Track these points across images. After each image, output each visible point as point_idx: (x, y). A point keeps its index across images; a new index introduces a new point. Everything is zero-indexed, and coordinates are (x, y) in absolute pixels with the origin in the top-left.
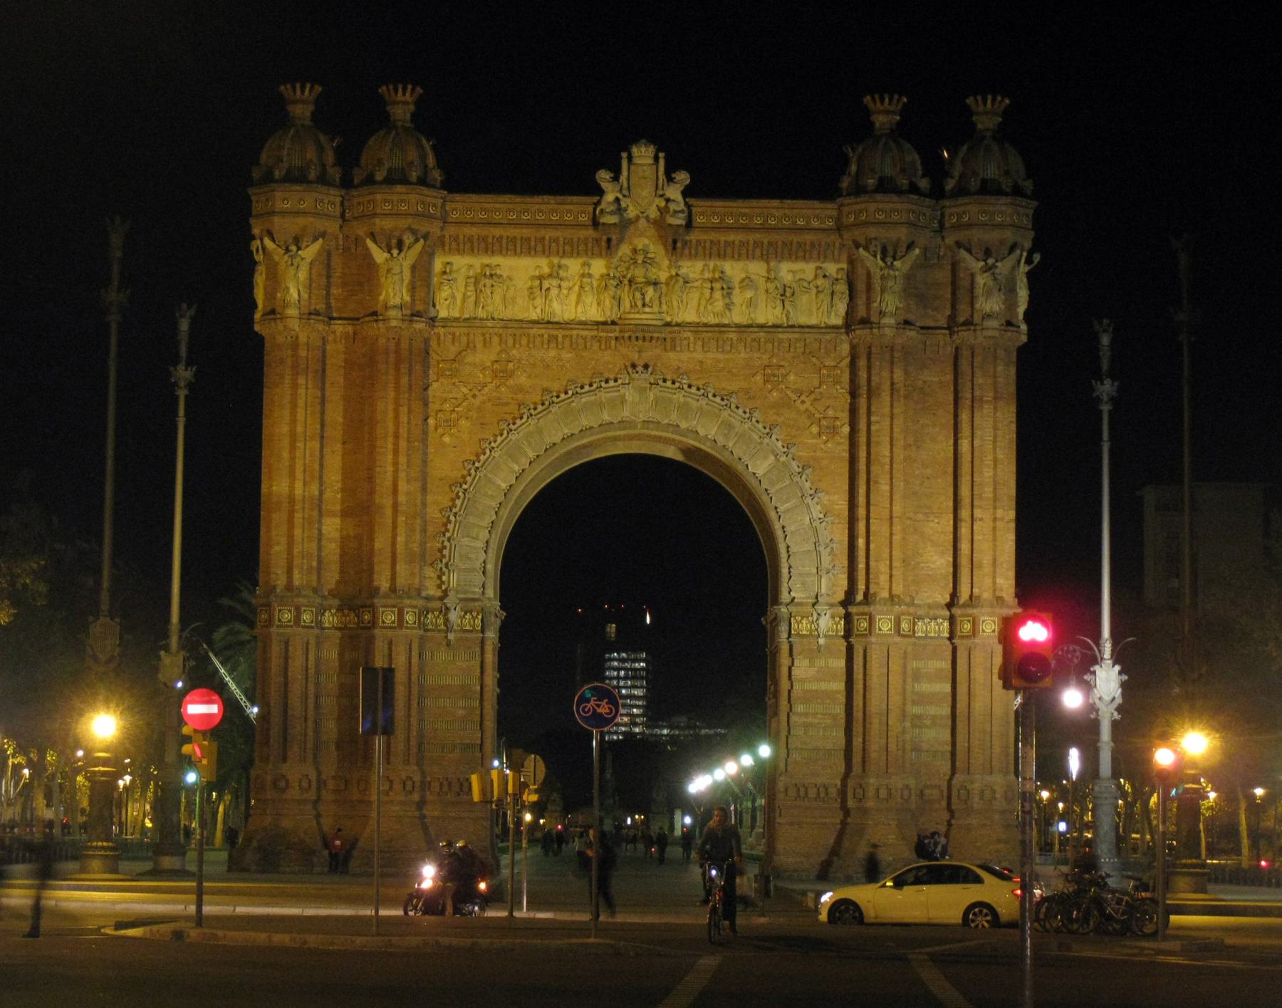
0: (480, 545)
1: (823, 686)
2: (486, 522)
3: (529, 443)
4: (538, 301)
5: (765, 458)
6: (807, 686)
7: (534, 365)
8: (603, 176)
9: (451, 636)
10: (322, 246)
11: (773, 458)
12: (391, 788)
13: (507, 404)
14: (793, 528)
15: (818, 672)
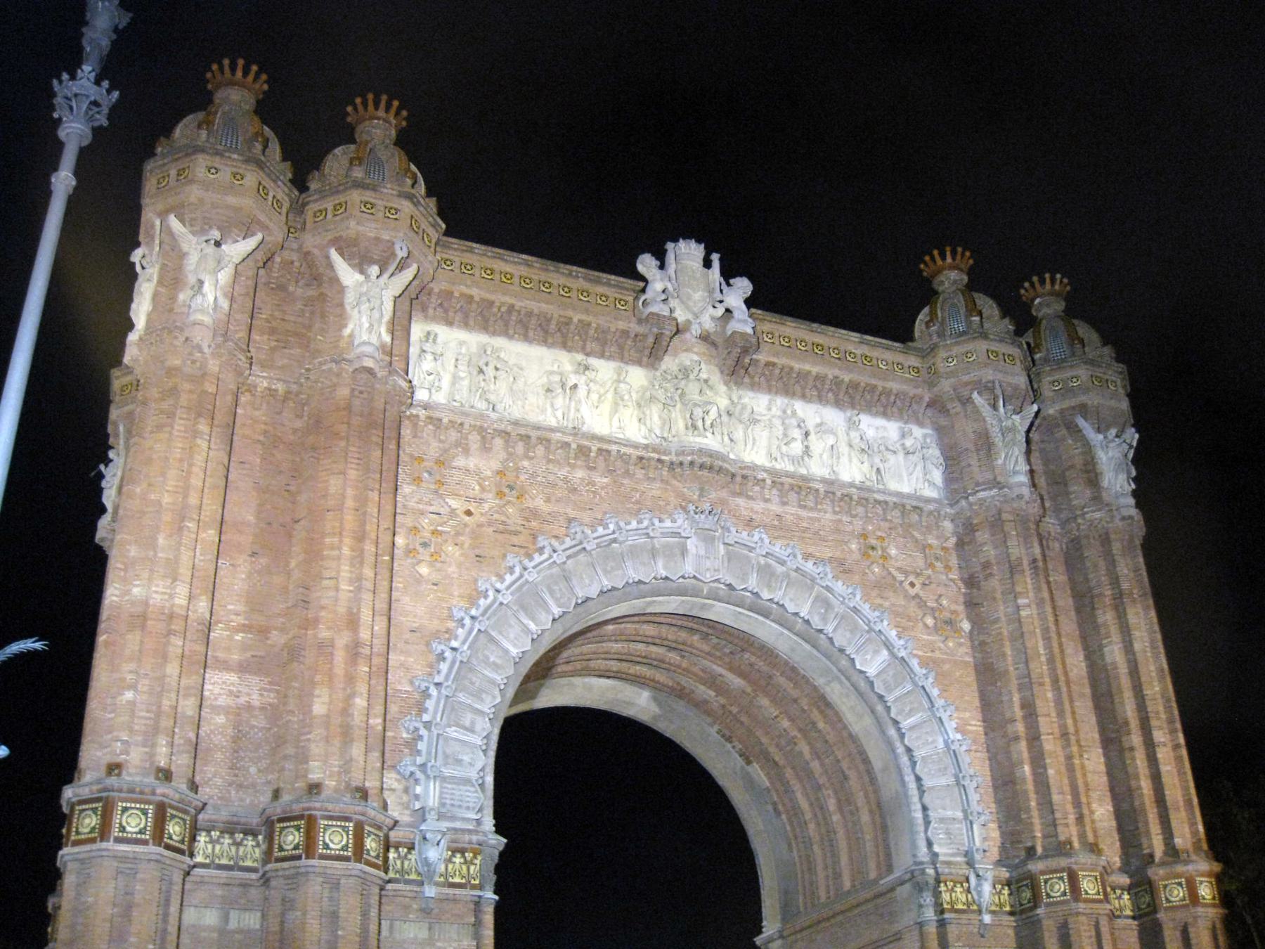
3: (552, 592)
4: (560, 401)
5: (876, 652)
7: (554, 485)
8: (646, 264)
9: (430, 891)
11: (885, 652)
13: (516, 533)
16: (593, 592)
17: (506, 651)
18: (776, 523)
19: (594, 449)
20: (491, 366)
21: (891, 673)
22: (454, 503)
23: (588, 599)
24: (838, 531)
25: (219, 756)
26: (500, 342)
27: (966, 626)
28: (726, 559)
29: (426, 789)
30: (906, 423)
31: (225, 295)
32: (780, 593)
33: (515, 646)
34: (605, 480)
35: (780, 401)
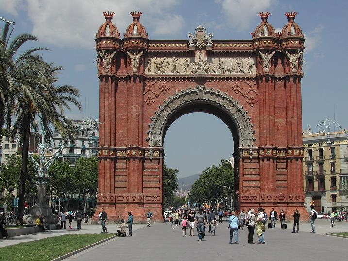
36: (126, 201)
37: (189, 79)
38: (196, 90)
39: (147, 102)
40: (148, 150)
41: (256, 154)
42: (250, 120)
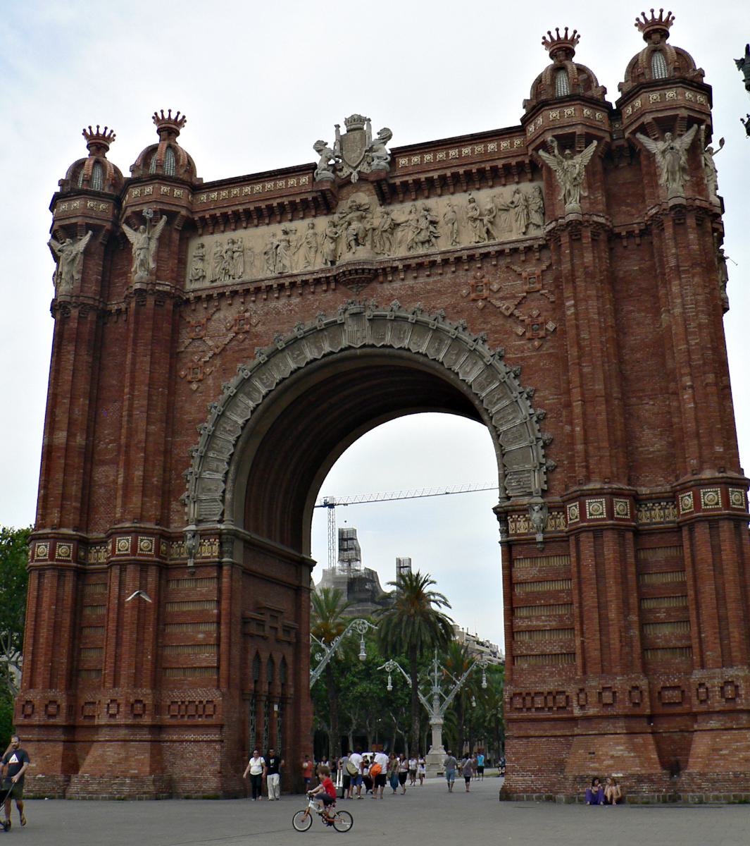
0: (220, 476)
1: (546, 587)
2: (226, 456)
3: (261, 380)
6: (528, 588)
10: (92, 237)
12: (118, 712)
14: (504, 428)
15: (540, 571)
16: (287, 374)
17: (236, 422)
18: (409, 293)
19: (287, 284)
20: (229, 253)
21: (485, 376)
22: (210, 343)
23: (284, 379)
24: (455, 285)
25: (102, 509)
26: (240, 234)
27: (551, 326)
28: (370, 329)
29: (190, 510)
30: (518, 183)
31: (78, 272)
32: (407, 341)
33: (241, 417)
34: (298, 300)
35: (420, 203)
36: (96, 722)
37: (317, 282)
38: (339, 319)
39: (189, 378)
40: (182, 537)
41: (559, 524)
42: (529, 397)
